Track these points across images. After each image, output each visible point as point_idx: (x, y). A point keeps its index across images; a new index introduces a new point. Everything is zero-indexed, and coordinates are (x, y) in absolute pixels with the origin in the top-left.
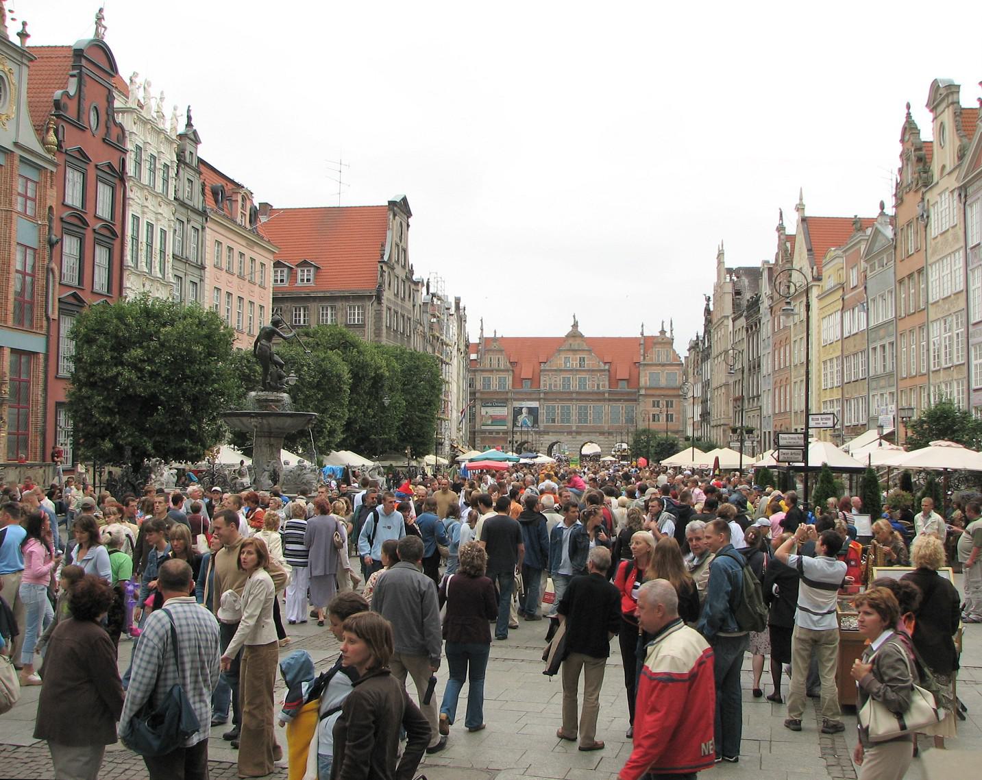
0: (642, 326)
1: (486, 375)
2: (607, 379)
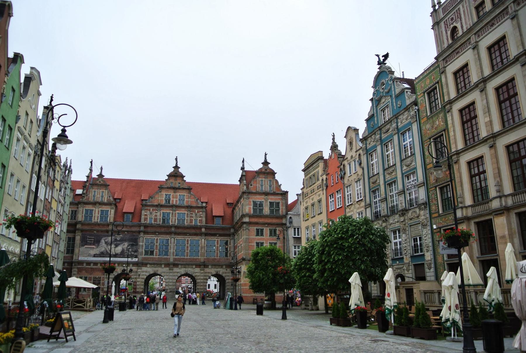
0: (243, 161)
1: (89, 207)
2: (204, 214)
